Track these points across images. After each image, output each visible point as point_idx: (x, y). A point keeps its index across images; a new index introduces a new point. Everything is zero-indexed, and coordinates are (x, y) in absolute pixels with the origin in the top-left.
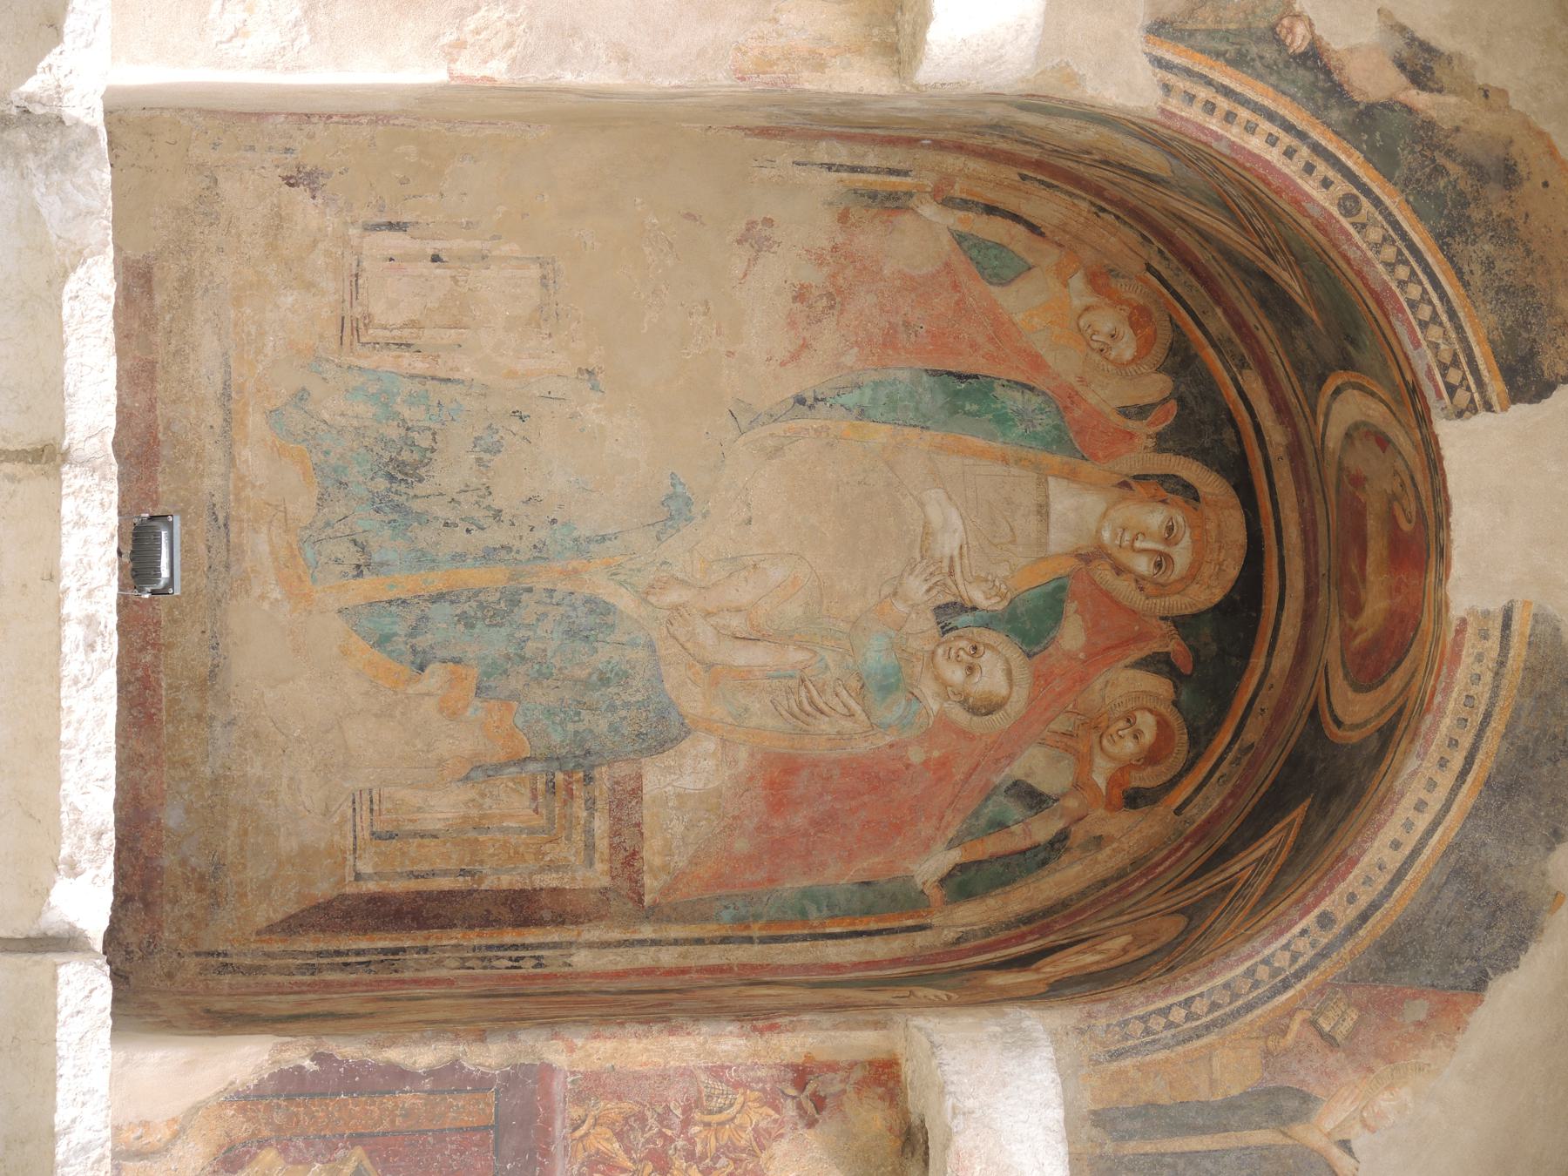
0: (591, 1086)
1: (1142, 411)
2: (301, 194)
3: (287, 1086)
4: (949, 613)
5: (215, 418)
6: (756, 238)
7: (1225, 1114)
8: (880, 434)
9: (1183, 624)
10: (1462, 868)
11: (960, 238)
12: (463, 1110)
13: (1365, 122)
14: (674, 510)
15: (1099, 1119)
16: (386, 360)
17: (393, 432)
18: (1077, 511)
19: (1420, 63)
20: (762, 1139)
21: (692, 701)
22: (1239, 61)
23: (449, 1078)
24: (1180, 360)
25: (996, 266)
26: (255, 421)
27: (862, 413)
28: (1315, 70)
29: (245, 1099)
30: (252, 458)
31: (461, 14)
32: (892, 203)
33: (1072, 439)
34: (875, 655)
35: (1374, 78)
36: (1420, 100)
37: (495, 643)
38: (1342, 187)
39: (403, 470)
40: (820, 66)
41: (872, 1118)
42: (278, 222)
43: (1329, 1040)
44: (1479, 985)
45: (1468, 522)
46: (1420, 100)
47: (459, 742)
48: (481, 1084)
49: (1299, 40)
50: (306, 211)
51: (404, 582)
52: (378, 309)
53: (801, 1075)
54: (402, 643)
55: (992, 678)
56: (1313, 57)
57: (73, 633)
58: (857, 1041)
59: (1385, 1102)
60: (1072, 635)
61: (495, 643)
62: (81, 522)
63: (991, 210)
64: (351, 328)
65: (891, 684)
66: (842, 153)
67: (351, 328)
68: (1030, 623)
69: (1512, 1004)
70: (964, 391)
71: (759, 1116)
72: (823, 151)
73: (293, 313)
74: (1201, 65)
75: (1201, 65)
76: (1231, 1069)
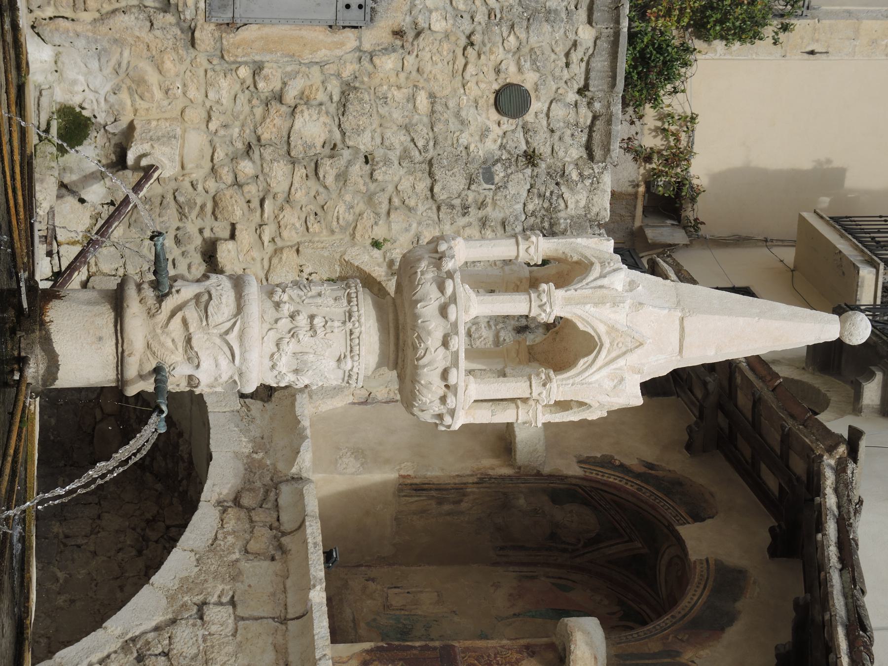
0: (466, 650)
1: (614, 614)
2: (370, 583)
3: (379, 649)
5: (352, 625)
6: (496, 586)
7: (654, 656)
8: (540, 620)
11: (553, 584)
13: (639, 476)
15: (616, 656)
16: (398, 612)
17: (400, 625)
19: (650, 466)
20: (518, 661)
22: (603, 467)
23: (424, 648)
26: (362, 625)
27: (533, 617)
28: (623, 468)
29: (368, 652)
31: (400, 464)
32: (533, 578)
36: (653, 472)
38: (636, 486)
40: (493, 469)
42: (365, 588)
43: (681, 640)
44: (722, 630)
46: (653, 472)
48: (435, 648)
49: (617, 463)
50: (372, 586)
52: (394, 603)
53: (527, 647)
57: (310, 546)
59: (701, 653)
62: (311, 526)
63: (560, 578)
66: (517, 569)
67: (387, 606)
69: (732, 633)
71: (516, 656)
72: (511, 569)
74: (592, 467)
75: (592, 467)
76: (654, 646)
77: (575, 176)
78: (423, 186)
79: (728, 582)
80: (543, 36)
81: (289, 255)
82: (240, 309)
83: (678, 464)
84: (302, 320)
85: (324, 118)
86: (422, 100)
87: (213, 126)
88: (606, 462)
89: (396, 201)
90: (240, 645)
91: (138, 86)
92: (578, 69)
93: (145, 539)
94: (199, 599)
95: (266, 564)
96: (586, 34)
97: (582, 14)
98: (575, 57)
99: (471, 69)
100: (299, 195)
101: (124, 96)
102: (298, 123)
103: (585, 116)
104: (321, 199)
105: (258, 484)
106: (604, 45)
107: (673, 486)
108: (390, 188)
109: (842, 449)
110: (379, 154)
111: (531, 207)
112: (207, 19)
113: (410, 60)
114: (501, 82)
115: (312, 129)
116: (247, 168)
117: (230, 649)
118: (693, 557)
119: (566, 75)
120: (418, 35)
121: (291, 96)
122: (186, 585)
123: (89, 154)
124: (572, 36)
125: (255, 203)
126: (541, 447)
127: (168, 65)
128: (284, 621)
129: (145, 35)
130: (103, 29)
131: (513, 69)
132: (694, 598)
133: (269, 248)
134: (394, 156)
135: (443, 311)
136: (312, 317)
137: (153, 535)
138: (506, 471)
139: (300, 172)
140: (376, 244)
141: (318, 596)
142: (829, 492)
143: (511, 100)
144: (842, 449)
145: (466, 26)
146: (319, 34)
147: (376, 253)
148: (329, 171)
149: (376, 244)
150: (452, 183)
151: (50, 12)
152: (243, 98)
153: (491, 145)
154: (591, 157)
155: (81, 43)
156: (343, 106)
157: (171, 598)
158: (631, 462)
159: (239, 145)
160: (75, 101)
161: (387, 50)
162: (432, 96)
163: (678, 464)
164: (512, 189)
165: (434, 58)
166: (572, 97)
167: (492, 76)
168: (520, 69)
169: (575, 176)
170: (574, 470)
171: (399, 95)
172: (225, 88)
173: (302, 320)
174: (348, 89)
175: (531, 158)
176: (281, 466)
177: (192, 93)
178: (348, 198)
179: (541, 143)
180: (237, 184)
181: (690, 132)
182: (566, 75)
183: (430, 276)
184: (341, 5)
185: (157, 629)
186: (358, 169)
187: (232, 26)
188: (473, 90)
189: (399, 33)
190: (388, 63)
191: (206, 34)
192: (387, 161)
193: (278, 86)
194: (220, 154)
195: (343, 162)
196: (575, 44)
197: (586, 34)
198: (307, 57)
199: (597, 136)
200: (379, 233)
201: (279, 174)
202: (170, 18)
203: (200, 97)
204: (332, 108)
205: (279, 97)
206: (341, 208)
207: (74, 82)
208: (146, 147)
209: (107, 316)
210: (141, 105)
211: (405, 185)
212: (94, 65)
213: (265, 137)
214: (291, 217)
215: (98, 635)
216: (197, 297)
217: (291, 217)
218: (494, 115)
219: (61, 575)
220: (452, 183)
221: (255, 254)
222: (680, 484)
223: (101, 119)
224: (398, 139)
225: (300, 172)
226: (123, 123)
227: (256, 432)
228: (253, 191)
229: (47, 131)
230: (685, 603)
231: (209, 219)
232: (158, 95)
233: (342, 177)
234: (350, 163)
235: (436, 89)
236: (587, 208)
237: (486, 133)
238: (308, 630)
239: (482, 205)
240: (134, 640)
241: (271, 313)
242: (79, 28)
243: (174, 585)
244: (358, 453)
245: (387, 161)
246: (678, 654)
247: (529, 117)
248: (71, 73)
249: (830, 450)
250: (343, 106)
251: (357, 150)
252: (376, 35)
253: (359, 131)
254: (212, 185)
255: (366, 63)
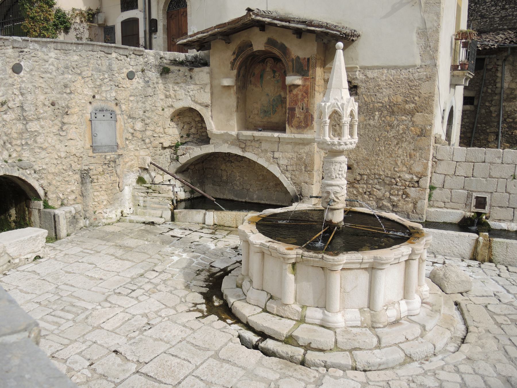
0: (289, 105)
3: (288, 123)
4: (274, 77)
6: (253, 90)
7: (293, 64)
9: (275, 62)
10: (279, 49)
12: (290, 112)
14: (268, 95)
18: (268, 69)
19: (234, 53)
21: (278, 94)
23: (288, 114)
24: (259, 62)
25: (254, 75)
28: (235, 60)
30: (264, 120)
32: (251, 81)
33: (264, 70)
34: (276, 82)
35: (235, 56)
37: (275, 106)
39: (265, 111)
41: (292, 87)
45: (259, 49)
47: (280, 109)
51: (271, 111)
53: (289, 92)
54: (275, 112)
55: (277, 74)
56: (234, 60)
58: (288, 87)
60: (275, 69)
61: (275, 106)
64: (258, 114)
65: (278, 81)
67: (258, 114)
68: (274, 72)
69: (287, 45)
70: (261, 77)
73: (257, 118)
76: (290, 64)
77: (146, 59)
78: (150, 98)
79: (271, 42)
80: (115, 66)
81: (166, 130)
82: (338, 186)
83: (234, 46)
84: (340, 173)
85: (137, 123)
86: (132, 98)
87: (139, 149)
88: (233, 64)
89: (153, 105)
90: (285, 152)
91: (131, 166)
92: (122, 57)
93: (229, 161)
94: (272, 159)
95: (262, 144)
96: (114, 55)
97: (109, 56)
98: (120, 58)
99: (124, 86)
100: (153, 128)
101: (134, 169)
102: (137, 129)
103: (133, 56)
104: (153, 123)
105: (238, 143)
106: (117, 50)
107: (240, 50)
108: (150, 106)
109: (251, 13)
110: (143, 109)
111: (154, 71)
112: (116, 152)
113: (122, 101)
114: (127, 78)
115: (139, 126)
116: (147, 141)
117: (286, 153)
118: (263, 49)
119: (123, 61)
120: (116, 99)
121: (132, 131)
122: (268, 160)
123: (146, 177)
124: (114, 59)
125: (154, 138)
126: (231, 79)
127: (127, 160)
128: (279, 142)
129: (121, 166)
130: (121, 176)
131: (123, 75)
132: (277, 52)
133: (164, 135)
134: (144, 105)
135: (346, 144)
136: (339, 171)
137: (228, 159)
138: (235, 88)
139: (148, 128)
140: (163, 110)
141: (276, 135)
142: (264, 19)
143: (130, 76)
144: (251, 13)
145: (114, 87)
146: (118, 124)
147: (166, 110)
148: (147, 121)
149: (163, 110)
150: (150, 91)
151: (118, 188)
152: (133, 142)
153: (141, 81)
154: (142, 55)
155: (124, 180)
156: (134, 118)
157: (271, 164)
158: (233, 58)
159: (142, 143)
160: (135, 180)
161: (121, 108)
162: (130, 96)
163: (234, 46)
164: (150, 76)
165: (122, 95)
166: (128, 59)
167: (125, 80)
168: (123, 73)
169: (146, 59)
170: (235, 72)
171: (131, 105)
172: (131, 147)
173: (340, 173)
174: (130, 117)
175: (143, 71)
176: (233, 138)
177: (132, 154)
178: (153, 116)
179: (140, 68)
180: (151, 143)
181: (76, 10)
182: (123, 61)
183: (338, 147)
184: (111, 119)
185: (279, 167)
186: (147, 114)
187: (117, 146)
188: (129, 85)
189: (117, 104)
190: (124, 107)
191: (120, 152)
192: (145, 107)
193: (130, 134)
194: (144, 147)
195: (146, 118)
196: (117, 58)
197: (114, 55)
198: (123, 127)
199: (138, 53)
200: (160, 109)
201: (149, 133)
202: (117, 160)
203: (133, 152)
204: (134, 121)
205: (132, 134)
206: (155, 118)
207: (132, 181)
208: (147, 165)
209: (335, 212)
210: (135, 165)
211: (150, 102)
212: (128, 177)
213: (141, 137)
214: (157, 130)
215: (281, 179)
216: (334, 194)
217: (157, 130)
218: (134, 80)
219: (238, 178)
220: (150, 91)
221: (166, 138)
222: (240, 47)
223: (138, 174)
224: (140, 104)
225: (148, 128)
226: (139, 169)
227: (221, 142)
228: (152, 139)
229: (148, 187)
230: (278, 54)
231: (158, 149)
232: (133, 162)
233: (149, 118)
234: (146, 116)
235: (129, 95)
236: (153, 56)
237: (138, 82)
238: (284, 138)
239: (154, 83)
240: (282, 172)
241: (338, 179)
242: (121, 181)
243: (267, 163)
244: (228, 120)
245: (145, 107)
246: (293, 59)
247: (134, 71)
248: (130, 182)
249: (250, 16)
250: (134, 118)
251: (143, 115)
252: (117, 110)
253: (139, 114)
254: (151, 148)
255: (124, 113)
